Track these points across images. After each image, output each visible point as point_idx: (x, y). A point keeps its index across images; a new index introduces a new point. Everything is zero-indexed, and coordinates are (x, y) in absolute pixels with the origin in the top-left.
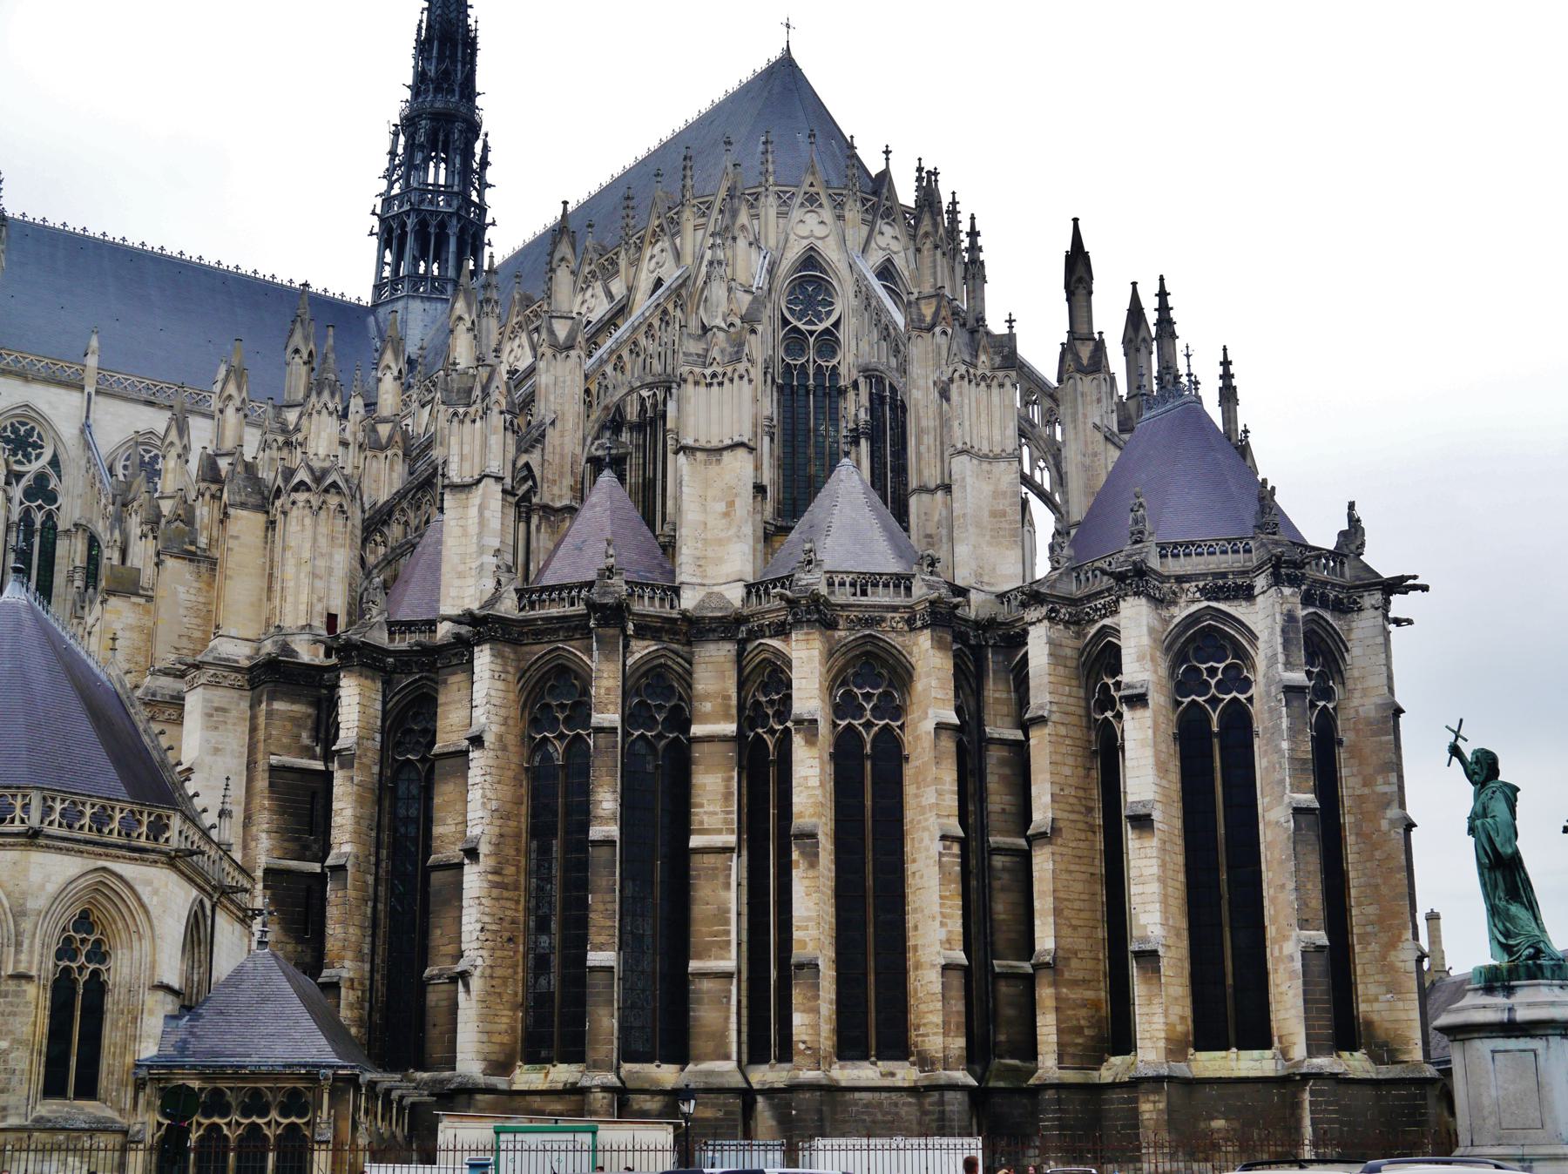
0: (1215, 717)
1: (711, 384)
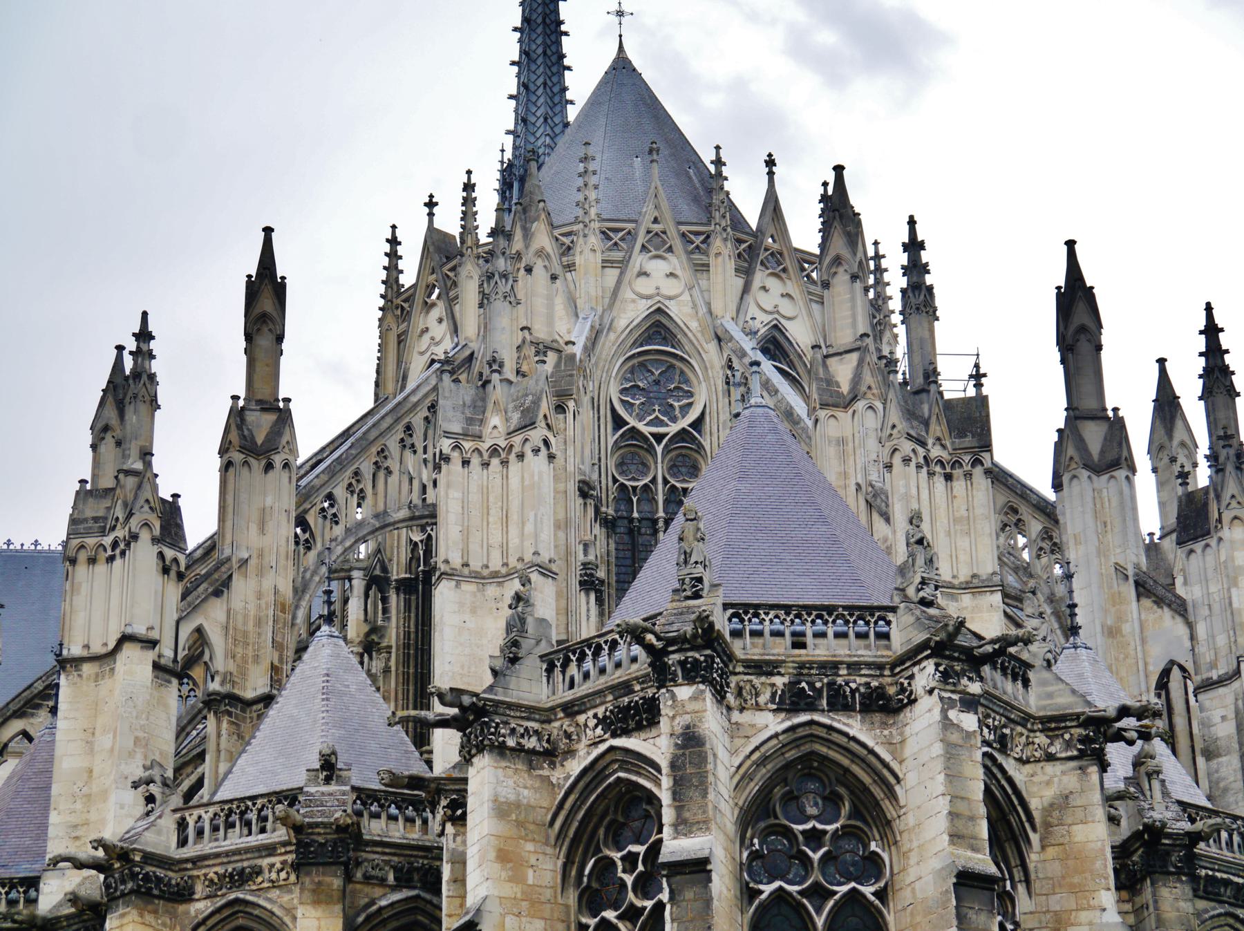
1: (111, 559)
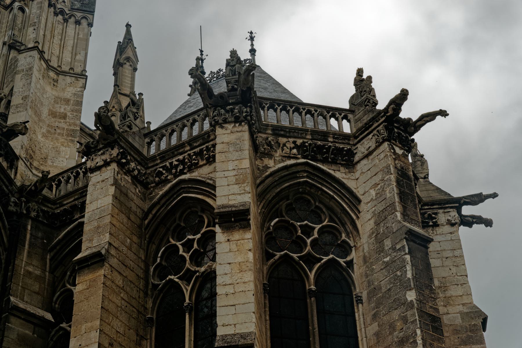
0: (312, 276)
